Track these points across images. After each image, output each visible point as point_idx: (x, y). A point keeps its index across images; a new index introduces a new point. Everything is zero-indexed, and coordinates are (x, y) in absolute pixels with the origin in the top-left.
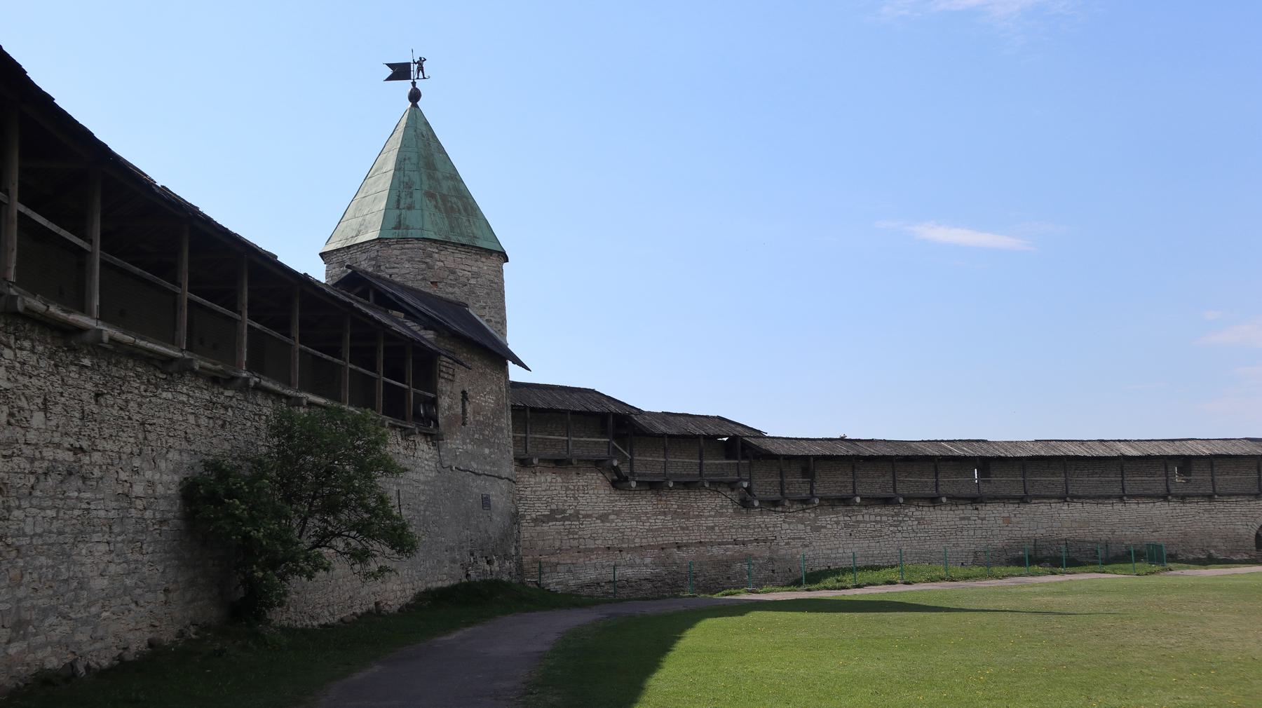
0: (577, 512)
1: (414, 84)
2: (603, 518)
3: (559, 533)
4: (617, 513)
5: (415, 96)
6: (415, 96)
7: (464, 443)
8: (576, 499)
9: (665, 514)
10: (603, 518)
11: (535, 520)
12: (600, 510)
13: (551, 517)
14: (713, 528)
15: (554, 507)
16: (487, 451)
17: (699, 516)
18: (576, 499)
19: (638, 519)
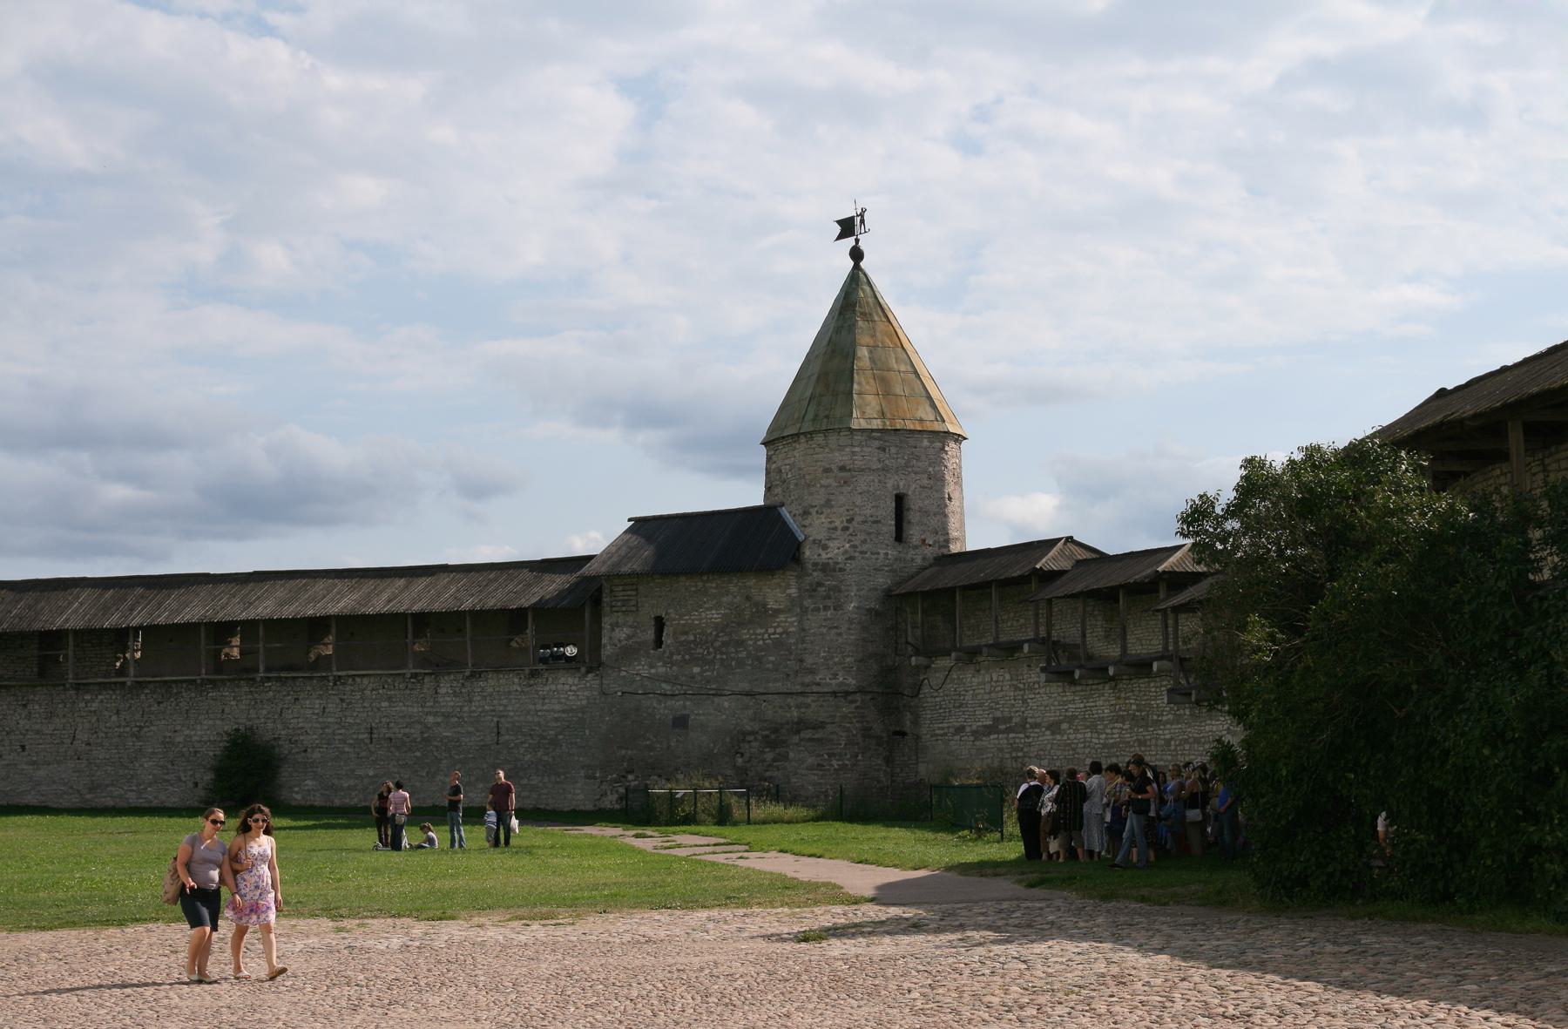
0: (1024, 720)
1: (857, 241)
2: (1054, 727)
3: (1001, 750)
4: (1070, 720)
5: (857, 254)
6: (857, 254)
7: (651, 666)
8: (1024, 701)
9: (1122, 719)
10: (1054, 727)
11: (976, 734)
12: (1051, 717)
13: (990, 730)
14: (1168, 742)
15: (998, 714)
16: (696, 670)
17: (1157, 723)
18: (1024, 701)
19: (1093, 727)
